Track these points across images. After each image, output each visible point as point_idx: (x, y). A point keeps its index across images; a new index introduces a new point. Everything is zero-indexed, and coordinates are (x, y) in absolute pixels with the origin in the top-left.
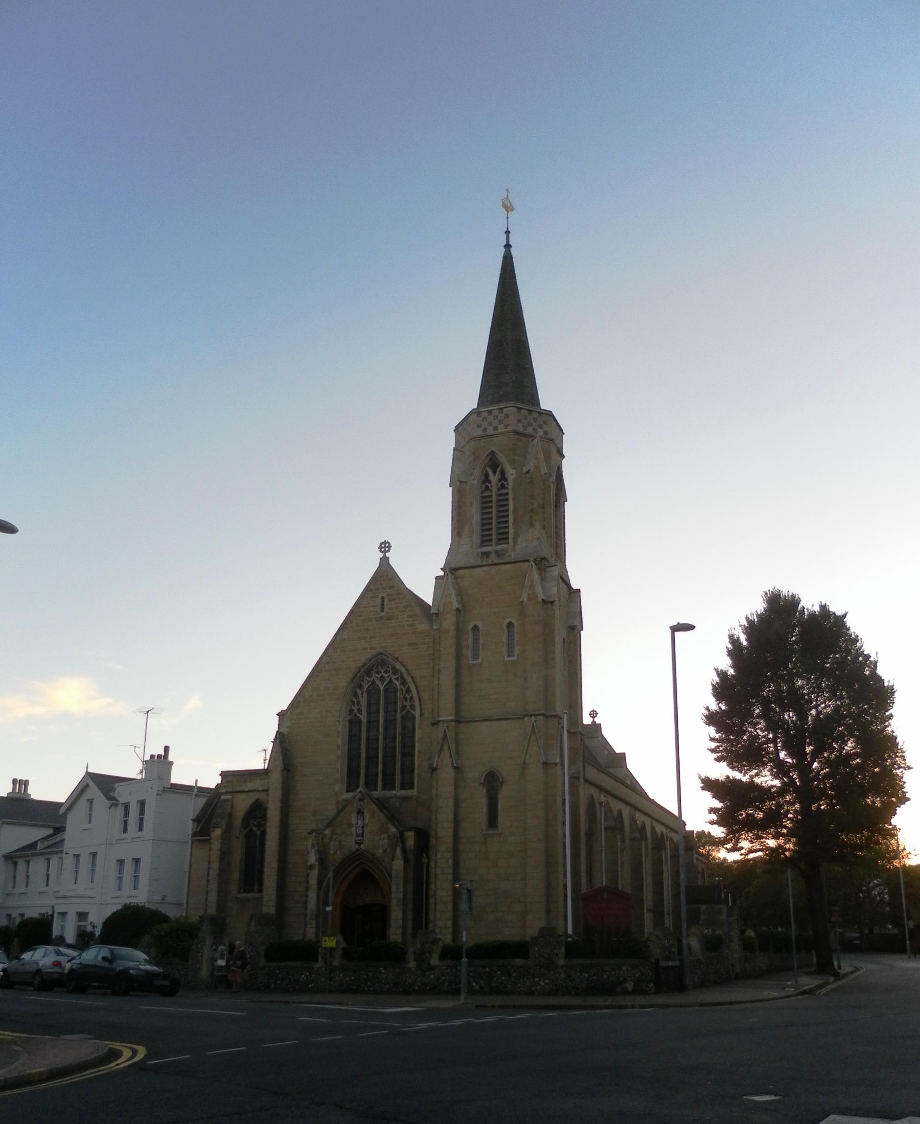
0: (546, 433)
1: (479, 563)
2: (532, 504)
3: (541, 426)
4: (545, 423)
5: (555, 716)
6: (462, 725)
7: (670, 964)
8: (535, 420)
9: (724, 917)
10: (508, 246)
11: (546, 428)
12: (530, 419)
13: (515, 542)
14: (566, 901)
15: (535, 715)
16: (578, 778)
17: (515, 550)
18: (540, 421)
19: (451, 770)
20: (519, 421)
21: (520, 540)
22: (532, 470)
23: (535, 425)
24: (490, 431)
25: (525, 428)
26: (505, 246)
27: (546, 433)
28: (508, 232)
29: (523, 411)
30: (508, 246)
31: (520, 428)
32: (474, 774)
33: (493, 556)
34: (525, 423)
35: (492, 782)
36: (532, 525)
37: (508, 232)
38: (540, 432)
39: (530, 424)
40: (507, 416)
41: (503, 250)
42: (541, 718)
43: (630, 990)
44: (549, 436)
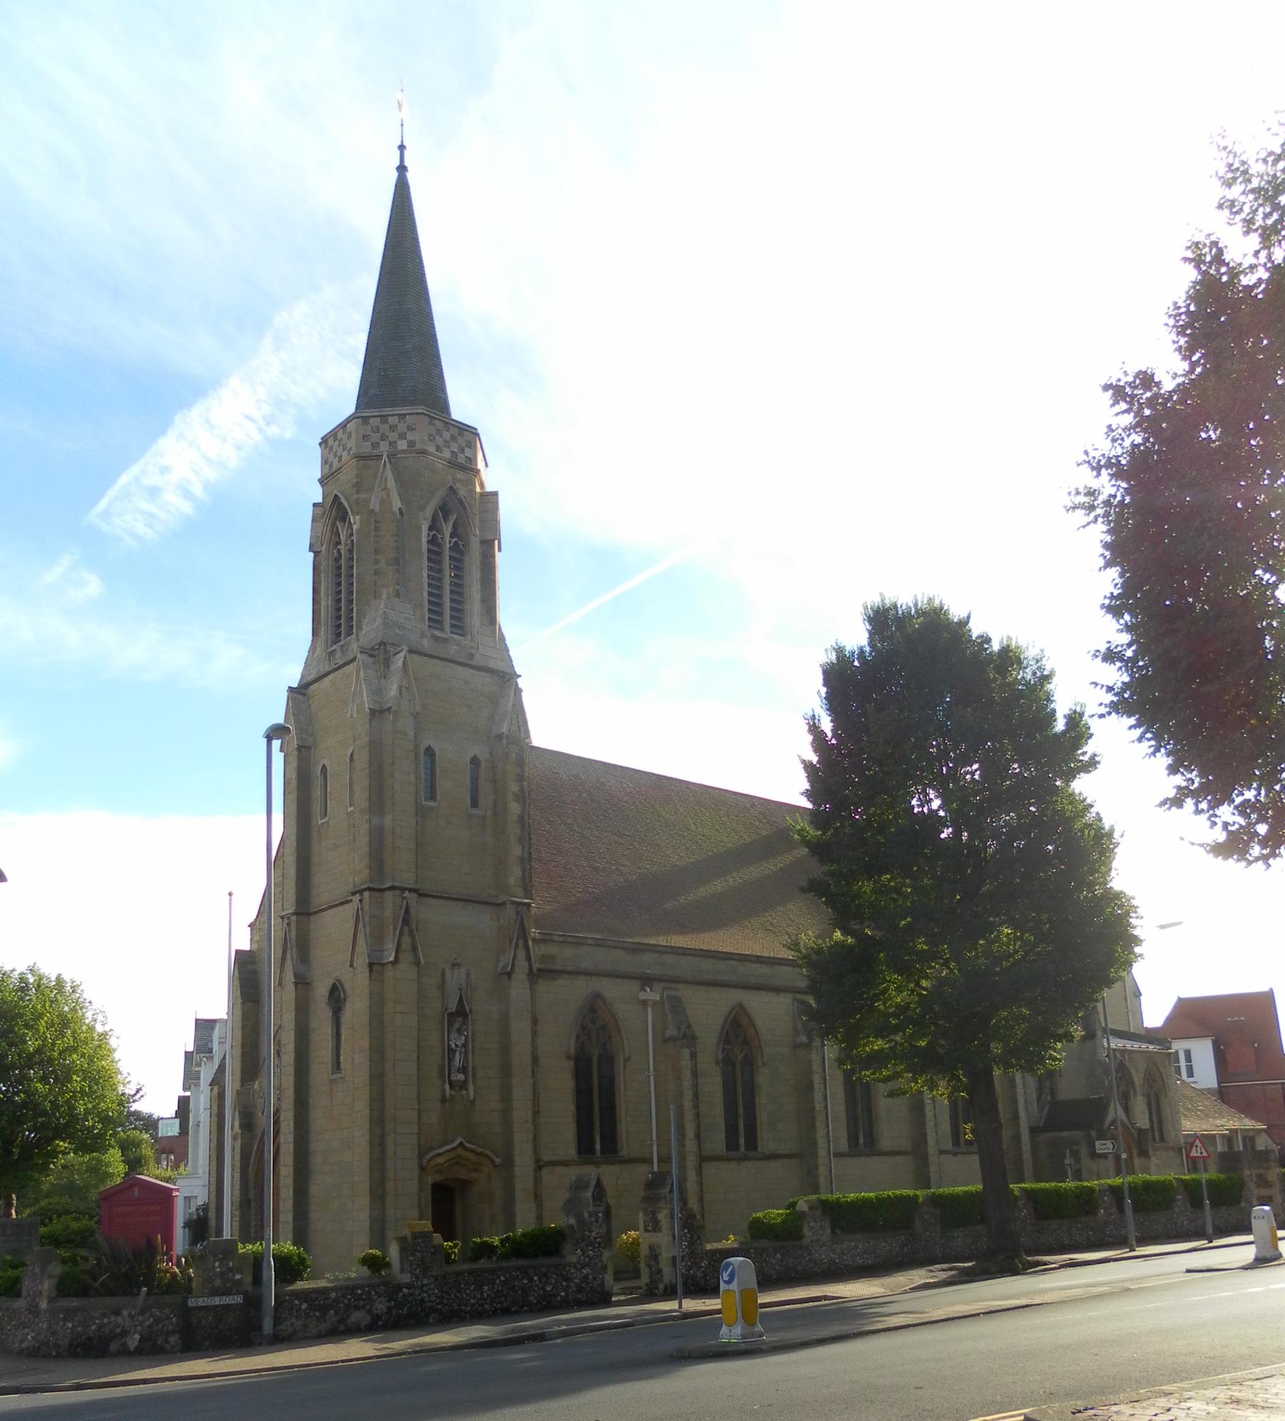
0: (411, 444)
1: (328, 669)
2: (377, 562)
3: (402, 436)
4: (410, 428)
5: (392, 888)
6: (312, 918)
7: (227, 1300)
8: (393, 428)
9: (589, 1194)
10: (402, 169)
11: (410, 436)
12: (384, 428)
13: (359, 628)
14: (276, 1188)
15: (361, 892)
16: (509, 974)
17: (358, 640)
18: (402, 427)
19: (293, 987)
20: (364, 437)
21: (365, 621)
22: (377, 509)
23: (393, 436)
24: (335, 465)
25: (375, 445)
26: (398, 169)
27: (411, 444)
28: (402, 148)
29: (371, 420)
30: (402, 169)
31: (366, 448)
32: (321, 990)
33: (338, 655)
34: (375, 437)
35: (337, 997)
36: (376, 595)
37: (402, 148)
38: (402, 445)
39: (384, 438)
40: (350, 436)
41: (395, 175)
42: (367, 894)
43: (132, 1347)
44: (418, 446)
